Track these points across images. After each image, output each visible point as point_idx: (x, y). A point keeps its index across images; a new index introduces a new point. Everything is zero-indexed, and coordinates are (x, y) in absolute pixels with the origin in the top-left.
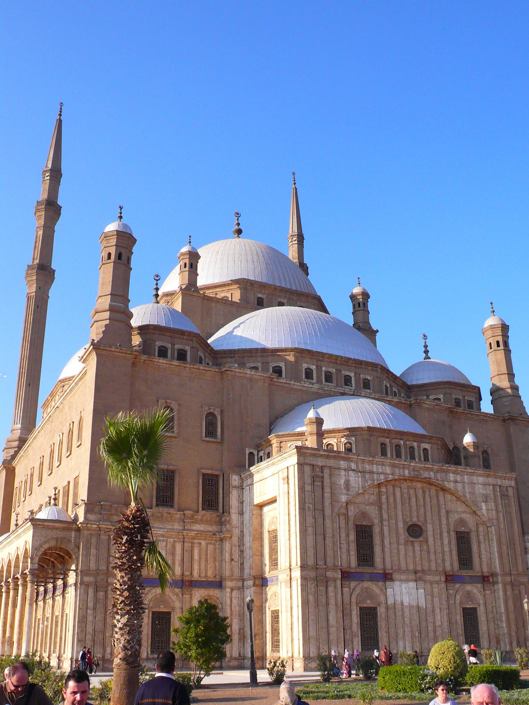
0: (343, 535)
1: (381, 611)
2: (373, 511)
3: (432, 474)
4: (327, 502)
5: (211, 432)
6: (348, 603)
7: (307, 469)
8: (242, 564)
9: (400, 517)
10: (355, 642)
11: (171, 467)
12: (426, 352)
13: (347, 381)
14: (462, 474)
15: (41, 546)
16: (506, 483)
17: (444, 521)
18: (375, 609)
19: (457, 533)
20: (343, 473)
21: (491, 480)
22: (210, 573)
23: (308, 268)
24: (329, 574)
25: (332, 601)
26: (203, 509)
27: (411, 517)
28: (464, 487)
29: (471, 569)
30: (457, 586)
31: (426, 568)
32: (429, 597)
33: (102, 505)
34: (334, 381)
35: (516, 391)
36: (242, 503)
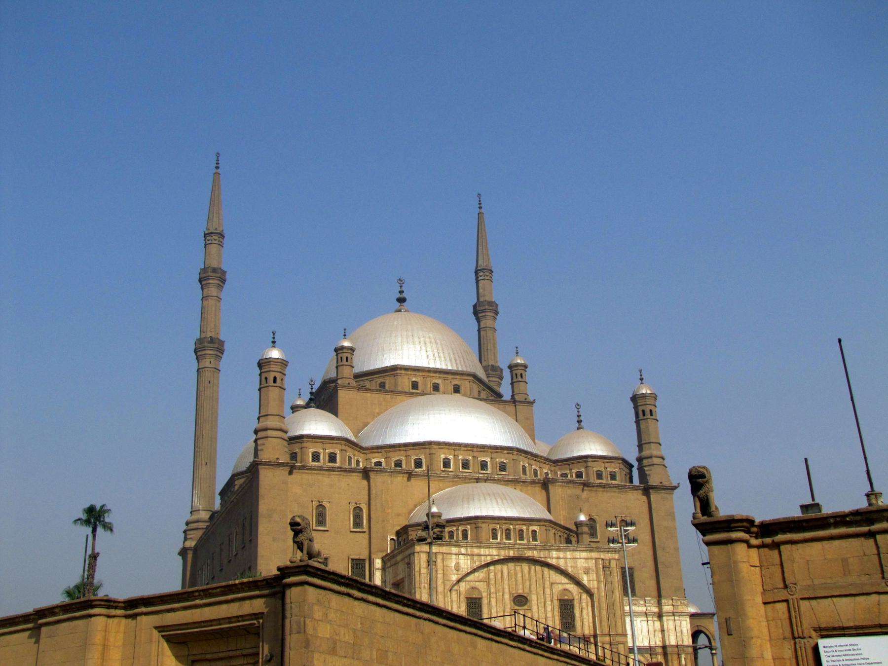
2: (482, 586)
3: (536, 553)
4: (440, 582)
7: (424, 557)
9: (507, 590)
12: (579, 422)
13: (484, 466)
16: (609, 556)
17: (548, 591)
20: (454, 557)
21: (594, 555)
23: (497, 305)
27: (517, 589)
28: (566, 563)
29: (574, 631)
34: (471, 468)
35: (661, 460)
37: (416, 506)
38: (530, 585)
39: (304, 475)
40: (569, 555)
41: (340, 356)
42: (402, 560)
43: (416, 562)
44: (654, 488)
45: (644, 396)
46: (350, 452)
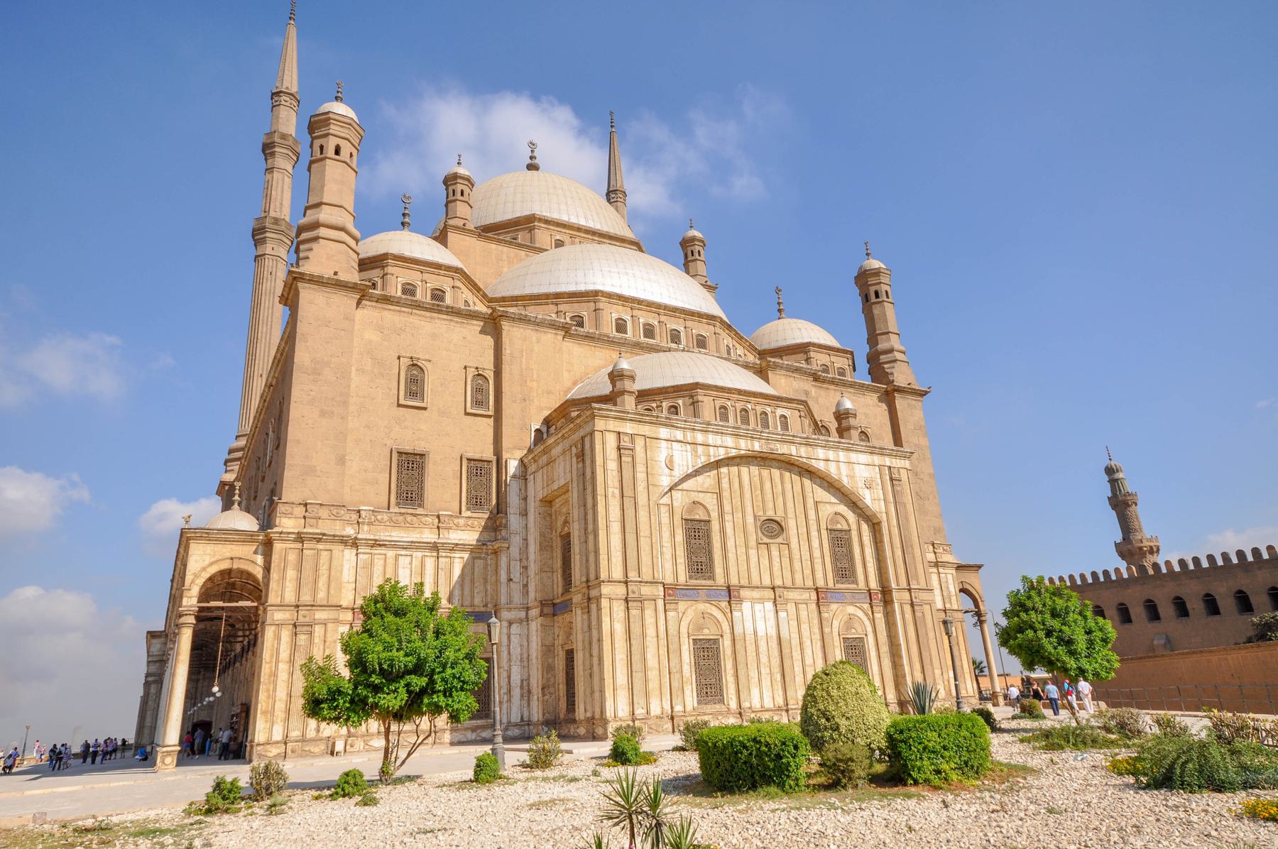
0: (666, 535)
1: (726, 644)
2: (710, 501)
3: (793, 450)
4: (641, 486)
5: (478, 403)
6: (676, 633)
7: (611, 440)
8: (526, 586)
9: (749, 510)
10: (688, 692)
11: (419, 450)
13: (675, 337)
14: (836, 448)
15: (204, 569)
17: (812, 514)
18: (716, 641)
19: (831, 531)
21: (877, 459)
22: (477, 601)
24: (646, 590)
25: (651, 631)
26: (468, 509)
29: (853, 583)
30: (834, 607)
31: (788, 583)
32: (794, 623)
33: (306, 505)
34: (657, 336)
36: (525, 499)
37: (575, 384)
38: (785, 504)
39: (386, 313)
40: (842, 455)
41: (451, 189)
42: (564, 452)
43: (598, 447)
44: (900, 390)
45: (877, 273)
46: (466, 294)
